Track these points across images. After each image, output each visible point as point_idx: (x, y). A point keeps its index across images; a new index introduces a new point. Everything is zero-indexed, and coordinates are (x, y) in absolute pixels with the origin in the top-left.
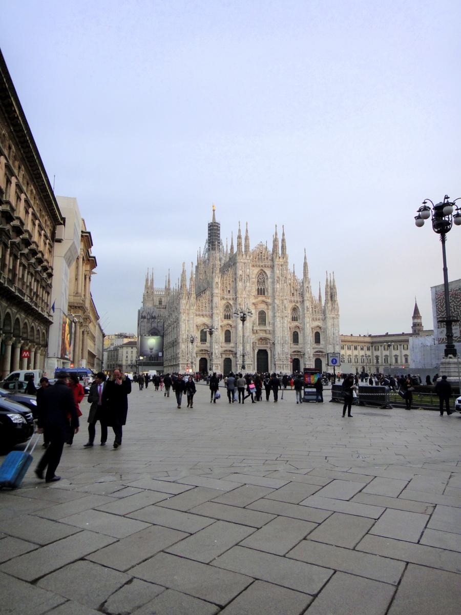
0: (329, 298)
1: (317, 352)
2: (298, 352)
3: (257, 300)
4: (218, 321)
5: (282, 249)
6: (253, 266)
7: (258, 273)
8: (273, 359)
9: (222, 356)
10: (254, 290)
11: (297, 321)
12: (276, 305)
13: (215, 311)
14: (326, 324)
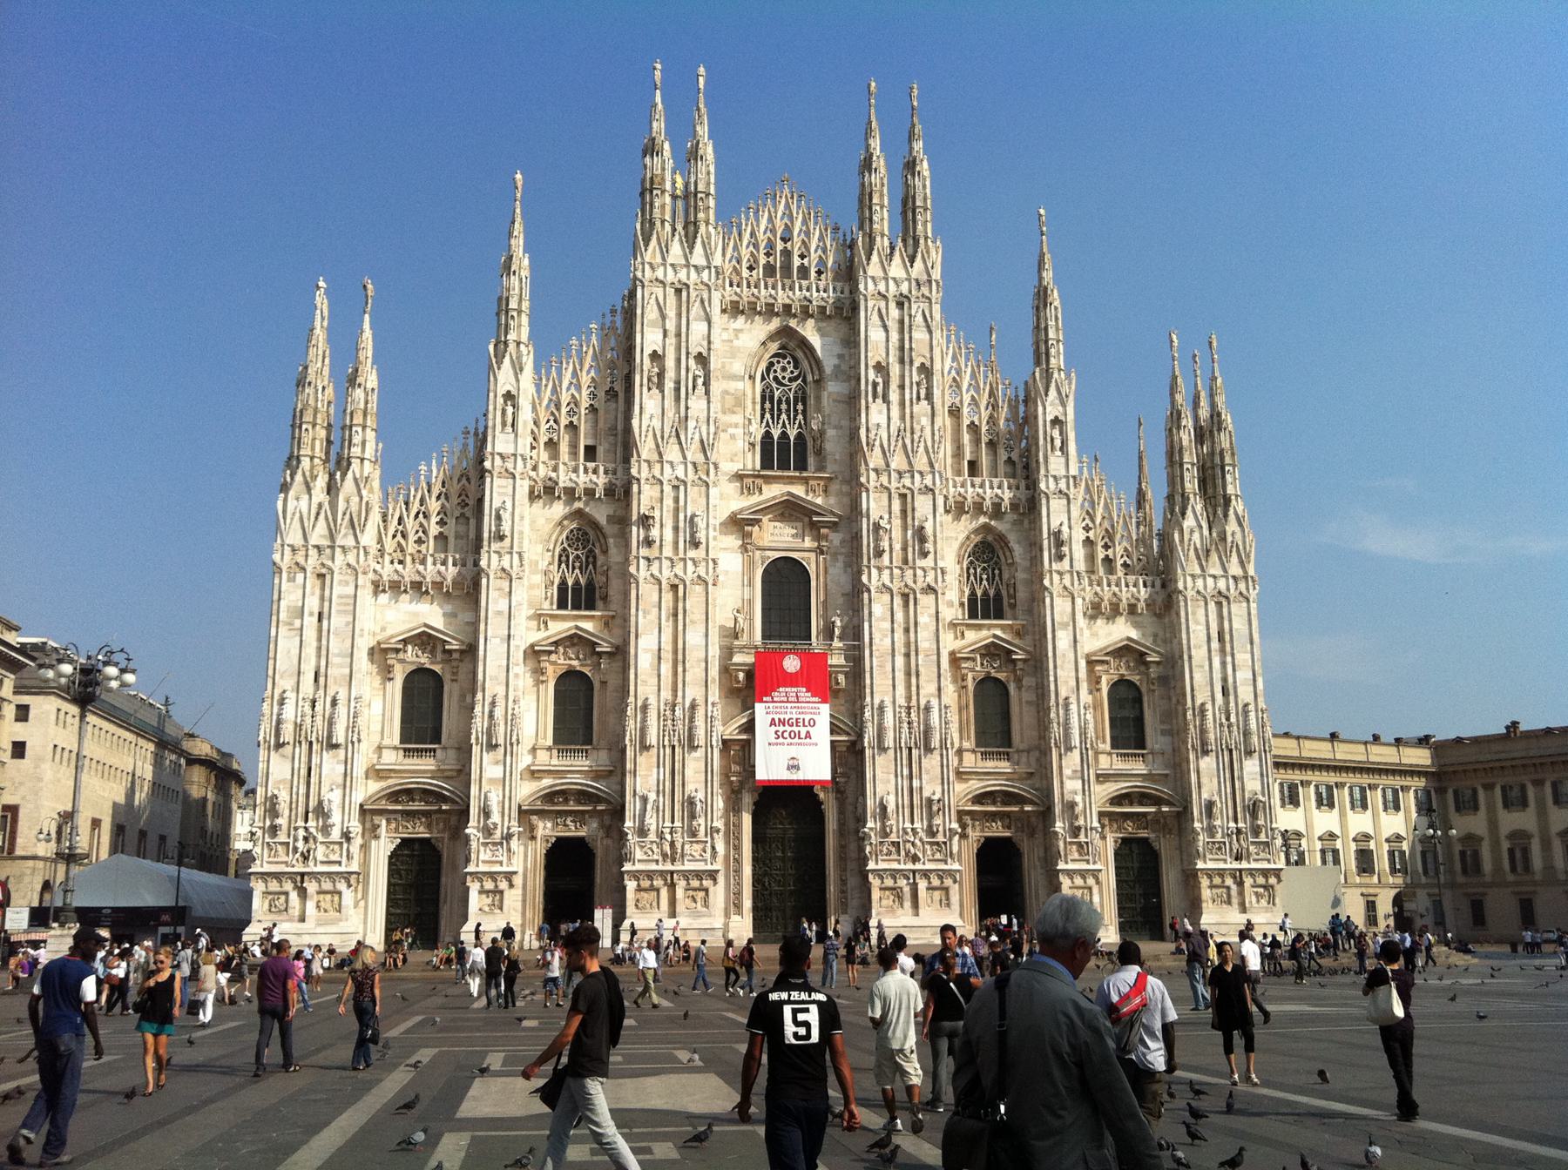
0: (1191, 484)
3: (755, 499)
6: (734, 310)
8: (853, 846)
9: (532, 828)
10: (741, 444)
11: (999, 615)
13: (490, 560)
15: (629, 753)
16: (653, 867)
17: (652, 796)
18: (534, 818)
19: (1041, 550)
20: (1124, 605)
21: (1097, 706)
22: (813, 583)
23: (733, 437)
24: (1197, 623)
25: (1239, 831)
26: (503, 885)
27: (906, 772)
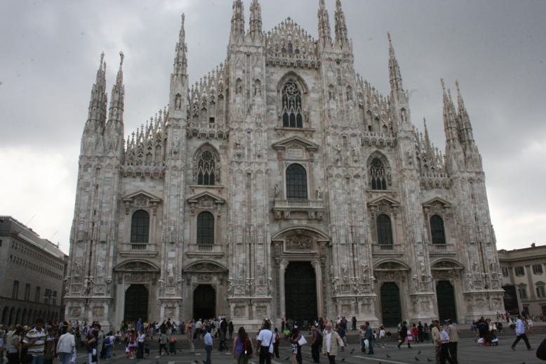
0: (456, 136)
2: (394, 265)
4: (179, 186)
5: (336, 31)
6: (270, 64)
7: (283, 78)
10: (275, 117)
11: (385, 188)
12: (329, 149)
13: (170, 163)
15: (230, 247)
16: (243, 297)
17: (241, 266)
18: (189, 275)
19: (401, 160)
21: (427, 226)
22: (308, 174)
23: (272, 114)
24: (463, 190)
25: (486, 275)
26: (176, 305)
27: (351, 254)
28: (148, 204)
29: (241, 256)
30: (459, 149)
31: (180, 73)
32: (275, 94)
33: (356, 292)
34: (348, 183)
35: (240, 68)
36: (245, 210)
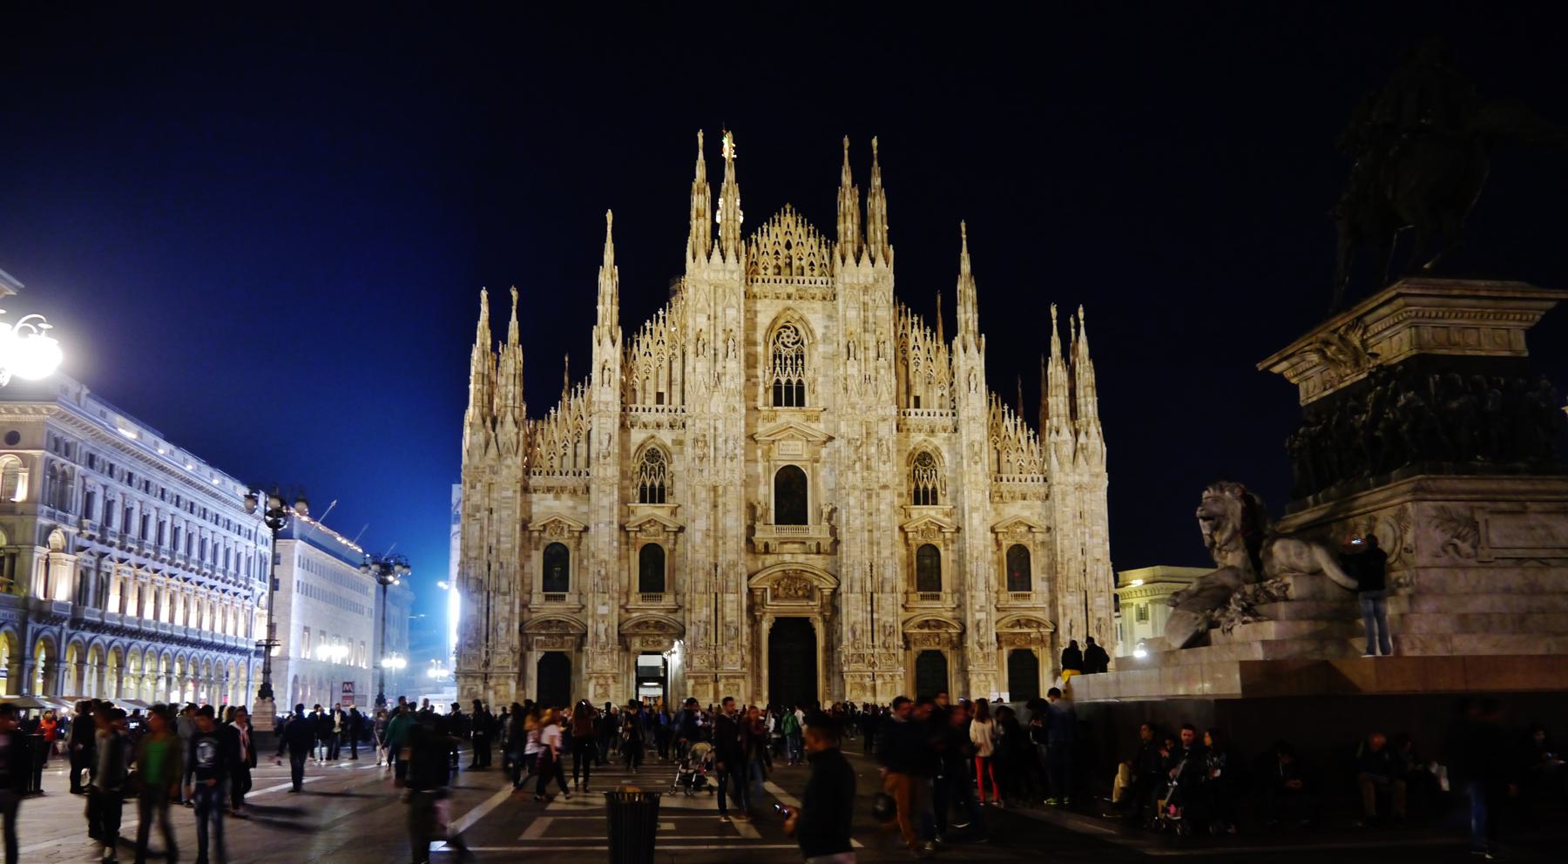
1: (1018, 623)
7: (775, 320)
10: (761, 389)
14: (1050, 511)
20: (1018, 495)
21: (999, 562)
28: (566, 535)
29: (703, 612)
30: (1066, 434)
31: (608, 323)
32: (760, 349)
33: (873, 665)
34: (870, 497)
35: (702, 311)
36: (710, 542)
